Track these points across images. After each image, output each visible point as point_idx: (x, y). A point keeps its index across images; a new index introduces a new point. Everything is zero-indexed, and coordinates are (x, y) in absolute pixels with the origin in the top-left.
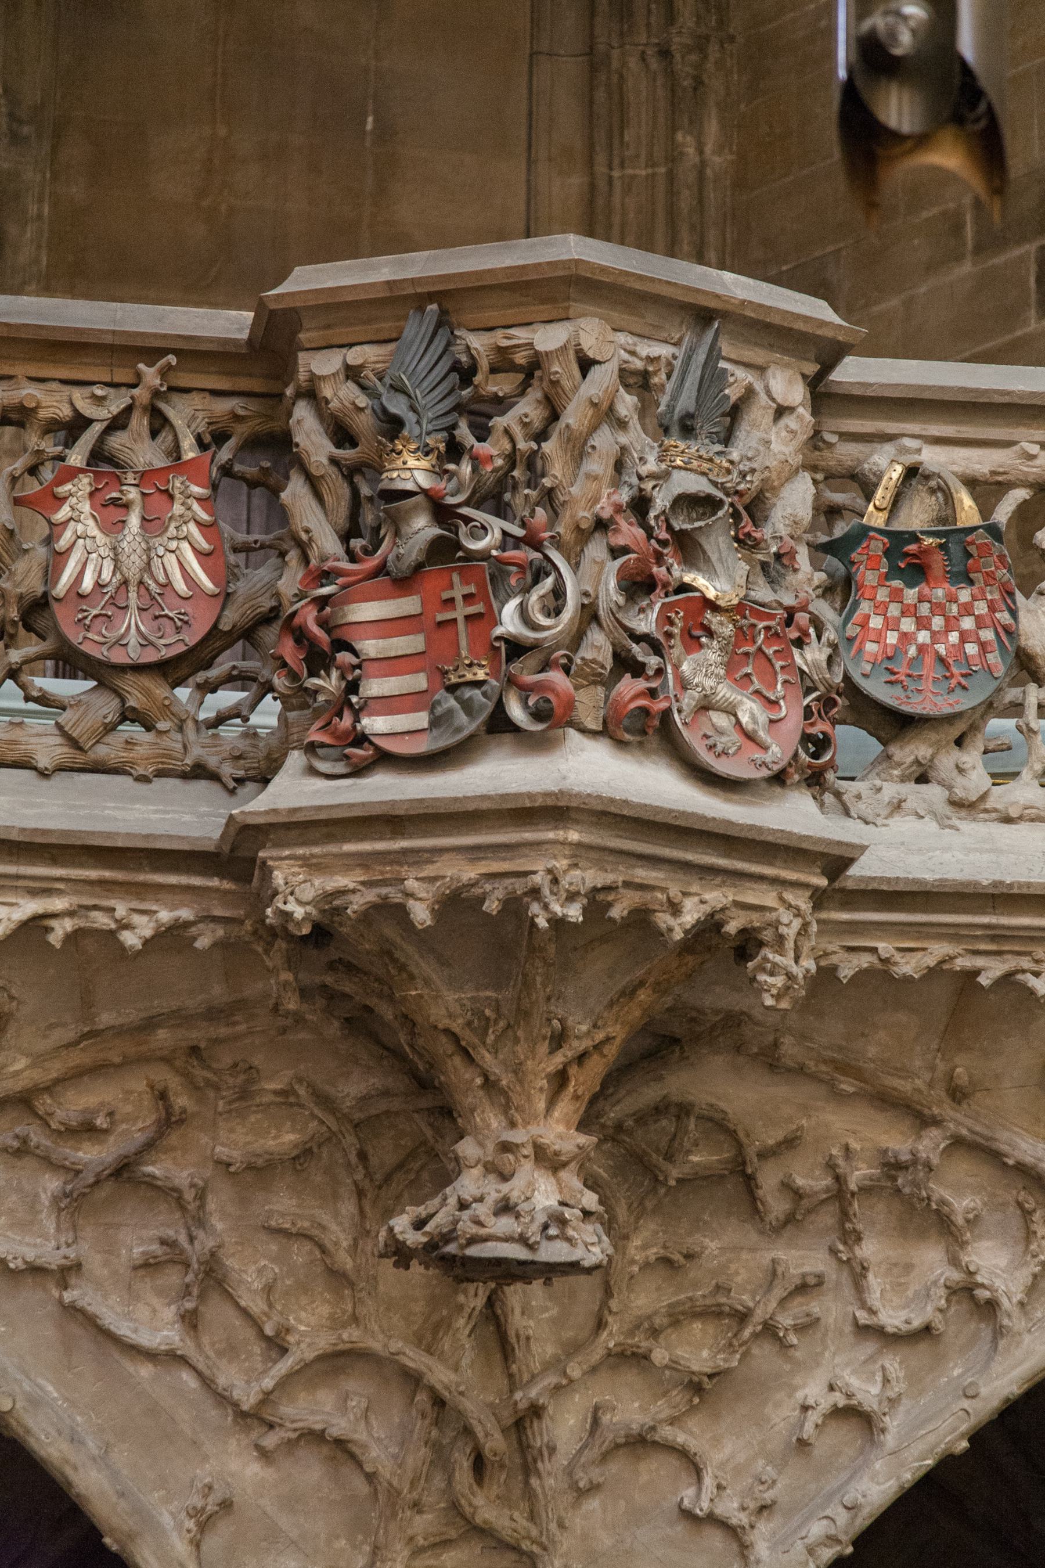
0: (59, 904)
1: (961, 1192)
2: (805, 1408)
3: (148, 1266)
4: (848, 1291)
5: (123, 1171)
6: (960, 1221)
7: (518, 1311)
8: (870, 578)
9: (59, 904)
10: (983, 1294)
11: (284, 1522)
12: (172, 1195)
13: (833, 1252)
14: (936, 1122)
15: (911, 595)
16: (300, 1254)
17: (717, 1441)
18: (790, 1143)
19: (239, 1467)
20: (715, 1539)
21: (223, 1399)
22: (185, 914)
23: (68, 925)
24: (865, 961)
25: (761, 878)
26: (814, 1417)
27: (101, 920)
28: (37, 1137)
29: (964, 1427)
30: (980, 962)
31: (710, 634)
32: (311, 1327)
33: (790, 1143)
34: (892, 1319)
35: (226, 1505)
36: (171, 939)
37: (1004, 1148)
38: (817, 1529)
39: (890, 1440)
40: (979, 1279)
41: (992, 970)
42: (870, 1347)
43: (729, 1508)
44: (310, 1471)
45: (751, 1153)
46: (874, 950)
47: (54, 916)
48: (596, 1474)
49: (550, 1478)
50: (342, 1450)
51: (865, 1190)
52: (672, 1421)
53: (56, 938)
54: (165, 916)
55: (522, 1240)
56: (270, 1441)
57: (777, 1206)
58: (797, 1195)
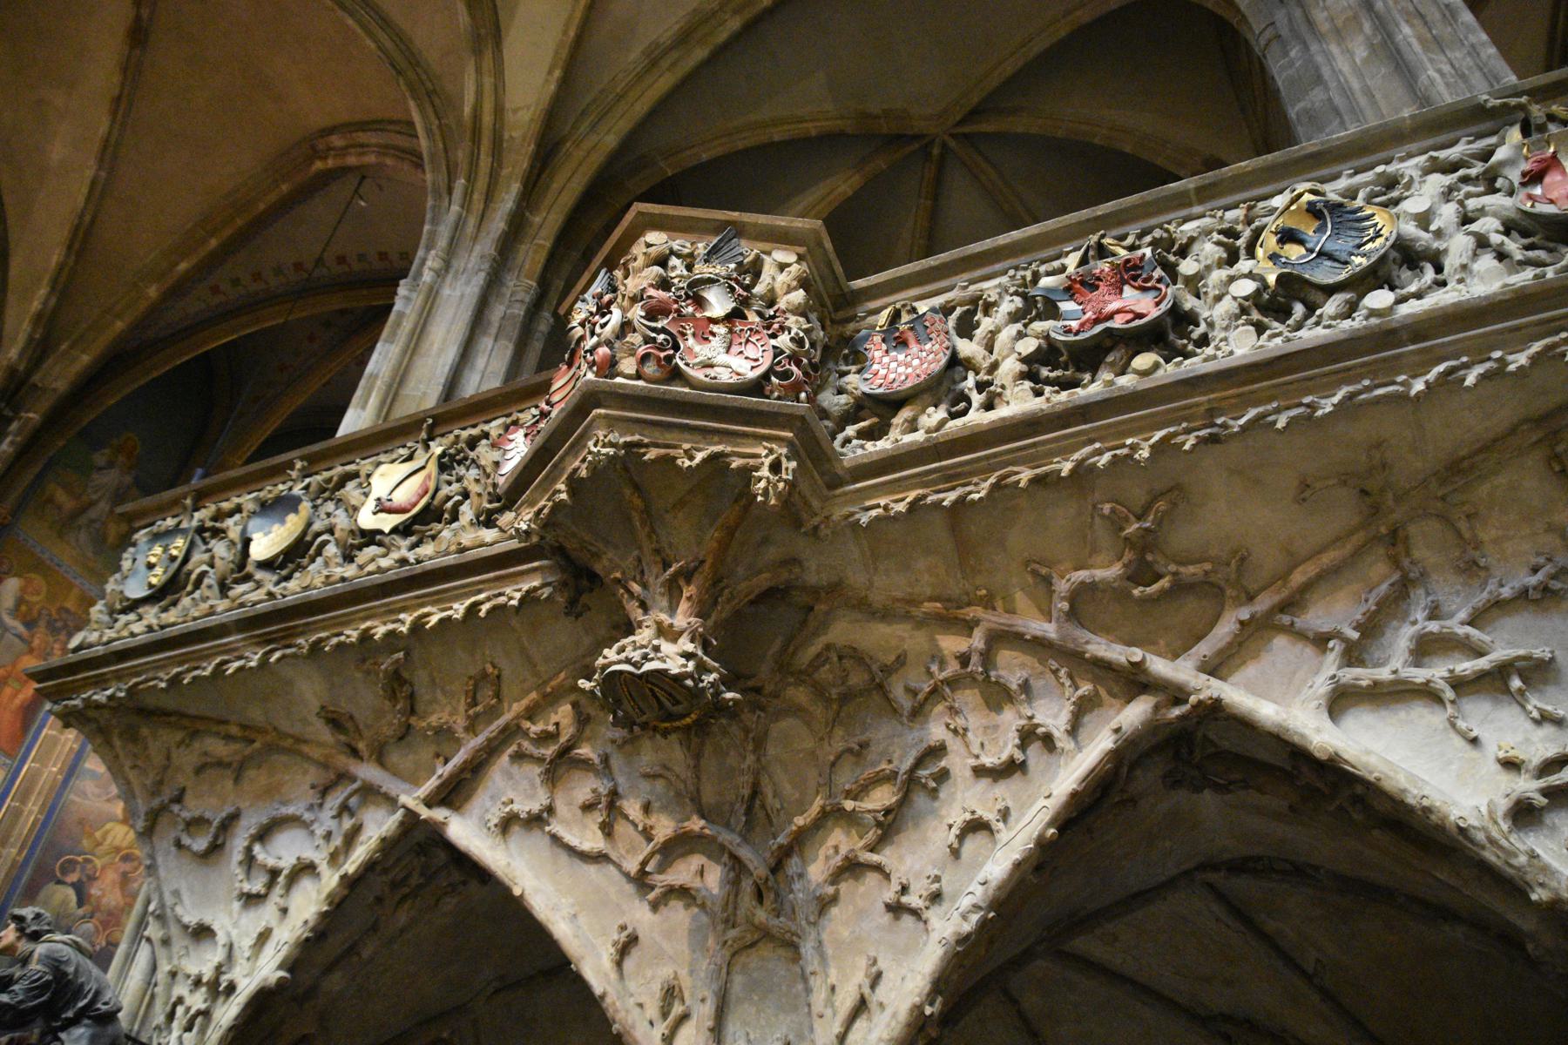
0: (482, 596)
1: (1012, 667)
2: (950, 826)
3: (588, 808)
4: (962, 750)
5: (565, 751)
6: (1014, 687)
7: (770, 795)
8: (878, 354)
9: (482, 596)
10: (1040, 730)
11: (666, 946)
12: (585, 764)
13: (947, 726)
14: (977, 622)
15: (901, 357)
16: (660, 785)
17: (901, 858)
18: (901, 660)
19: (640, 915)
20: (907, 920)
21: (627, 875)
22: (536, 583)
23: (485, 608)
24: (874, 513)
25: (745, 435)
26: (955, 831)
27: (502, 600)
28: (526, 744)
29: (1047, 818)
30: (941, 496)
31: (714, 334)
32: (664, 827)
33: (901, 660)
34: (988, 760)
35: (633, 940)
36: (529, 598)
37: (1021, 629)
38: (966, 902)
39: (1004, 835)
40: (1035, 721)
41: (951, 497)
42: (985, 783)
43: (912, 900)
44: (679, 915)
45: (875, 667)
46: (878, 506)
47: (482, 603)
48: (830, 890)
49: (799, 894)
50: (683, 893)
51: (953, 683)
52: (872, 849)
53: (482, 614)
54: (525, 587)
55: (628, 661)
56: (652, 896)
57: (906, 703)
58: (913, 692)
